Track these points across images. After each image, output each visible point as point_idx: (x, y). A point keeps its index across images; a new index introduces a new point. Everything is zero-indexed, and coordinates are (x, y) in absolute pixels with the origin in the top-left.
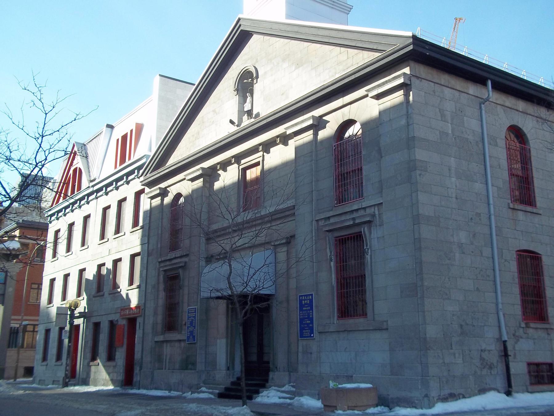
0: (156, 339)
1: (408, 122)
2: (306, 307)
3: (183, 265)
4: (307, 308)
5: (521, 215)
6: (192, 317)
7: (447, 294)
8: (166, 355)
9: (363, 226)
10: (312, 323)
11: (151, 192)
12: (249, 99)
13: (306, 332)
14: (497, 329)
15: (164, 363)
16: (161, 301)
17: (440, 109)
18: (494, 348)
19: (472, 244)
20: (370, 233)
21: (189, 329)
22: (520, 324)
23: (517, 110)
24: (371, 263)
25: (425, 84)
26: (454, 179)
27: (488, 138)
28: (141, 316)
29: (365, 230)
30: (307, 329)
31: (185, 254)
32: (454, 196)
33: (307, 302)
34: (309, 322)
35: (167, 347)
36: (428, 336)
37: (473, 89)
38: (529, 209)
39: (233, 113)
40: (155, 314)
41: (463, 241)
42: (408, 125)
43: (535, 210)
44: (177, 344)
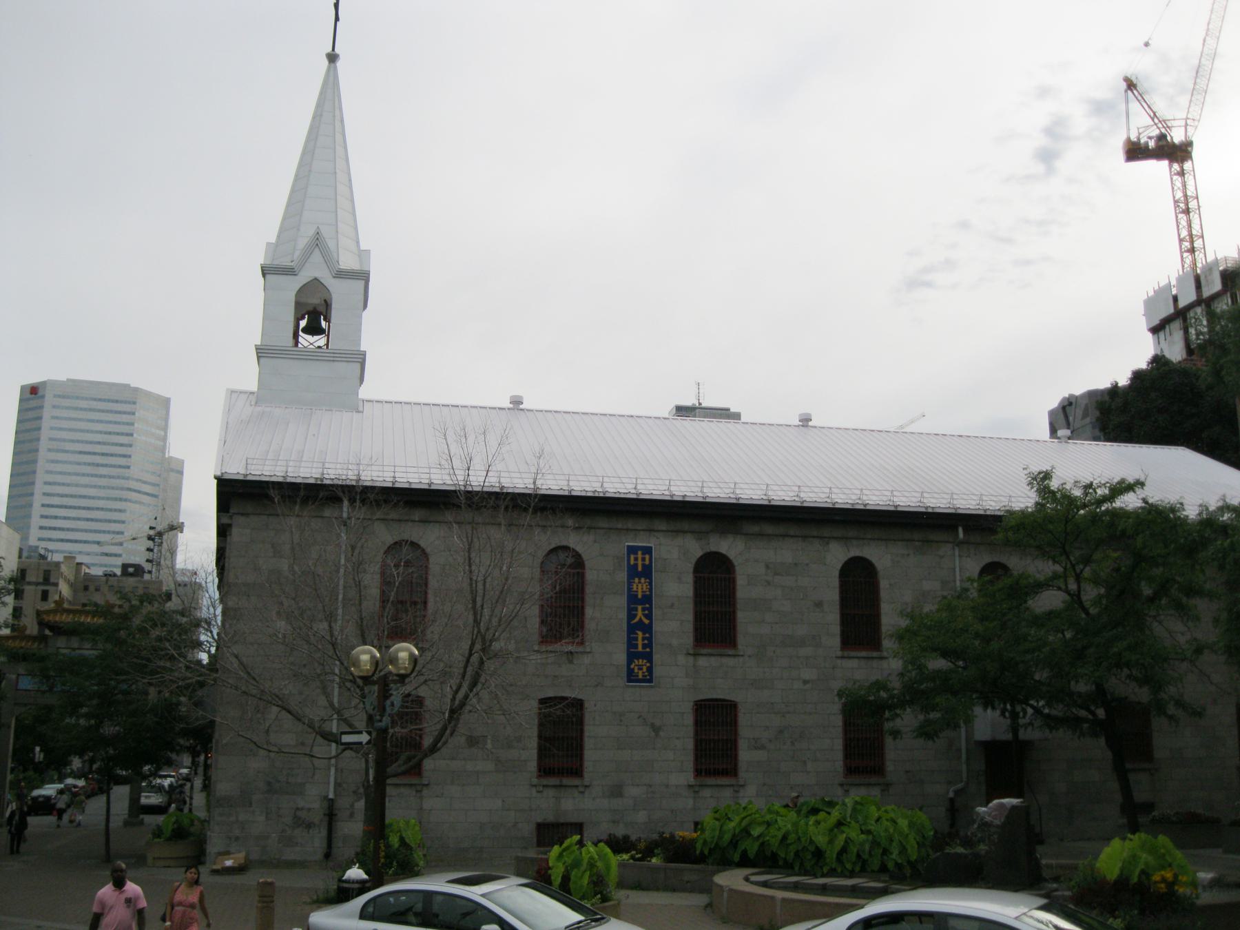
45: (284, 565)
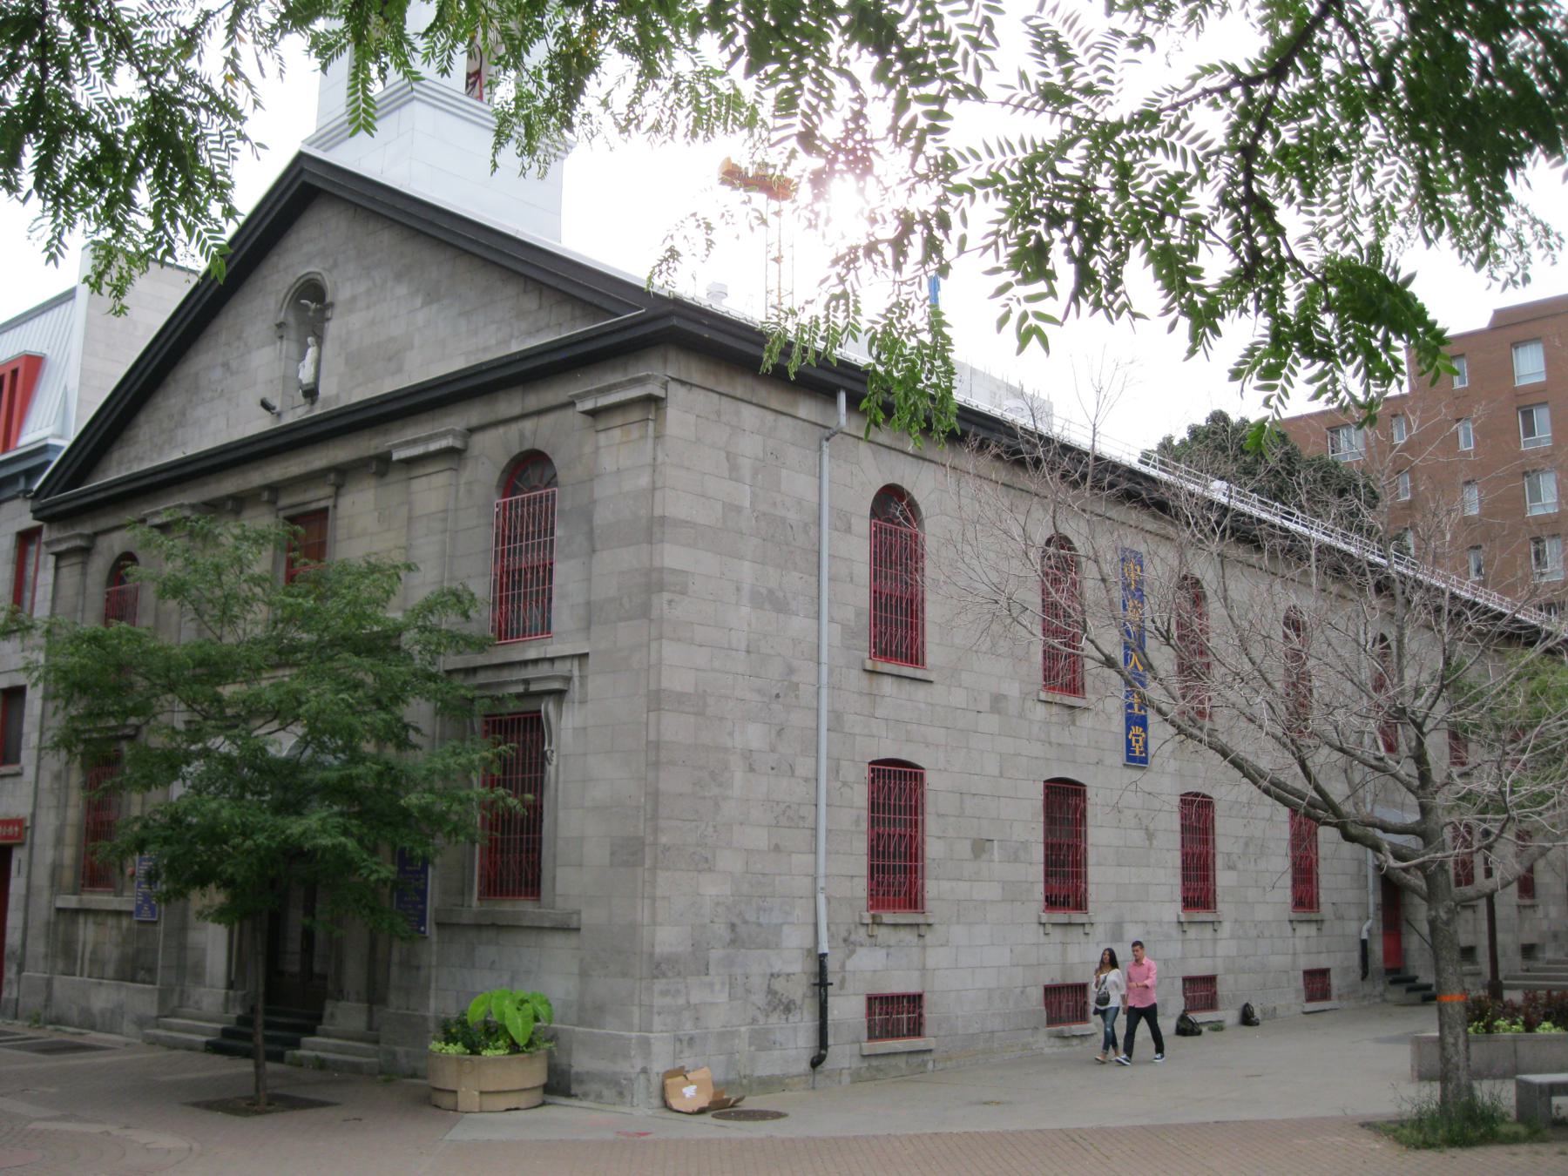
0: (60, 904)
1: (654, 482)
3: (132, 733)
5: (887, 685)
7: (706, 860)
9: (546, 699)
10: (424, 902)
11: (59, 541)
12: (311, 353)
14: (810, 929)
15: (79, 962)
16: (74, 814)
17: (728, 454)
18: (798, 967)
19: (773, 750)
20: (560, 715)
22: (861, 917)
23: (903, 452)
24: (557, 782)
25: (699, 397)
26: (745, 610)
27: (831, 515)
28: (22, 844)
29: (548, 708)
32: (743, 646)
35: (86, 923)
36: (658, 950)
37: (807, 409)
38: (907, 670)
39: (271, 381)
40: (59, 842)
41: (755, 745)
42: (654, 489)
43: (919, 673)
44: (111, 921)
45: (744, 497)
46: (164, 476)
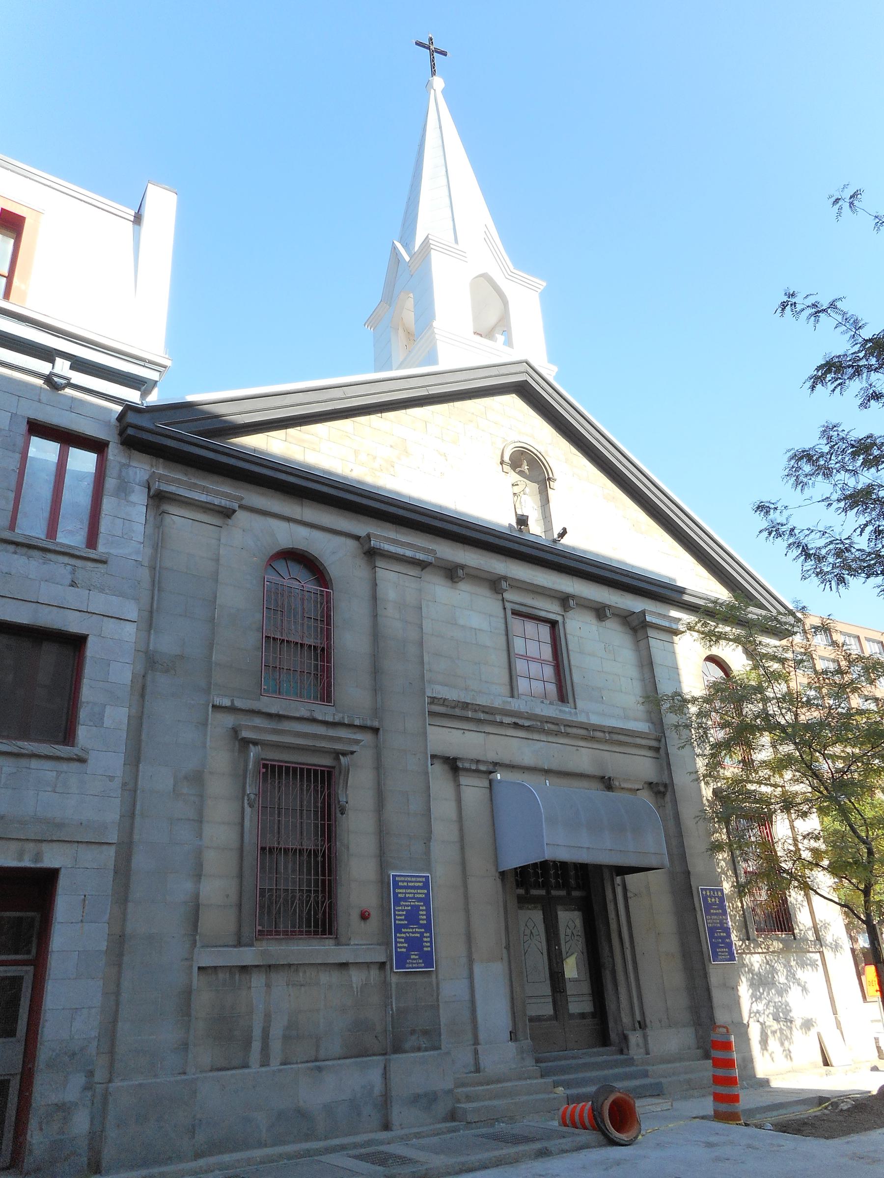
0: (206, 959)
2: (716, 909)
4: (718, 911)
6: (412, 898)
8: (268, 1017)
13: (723, 952)
15: (256, 1046)
21: (401, 932)
30: (722, 947)
31: (357, 723)
33: (715, 901)
34: (725, 934)
35: (268, 986)
46: (401, 512)
